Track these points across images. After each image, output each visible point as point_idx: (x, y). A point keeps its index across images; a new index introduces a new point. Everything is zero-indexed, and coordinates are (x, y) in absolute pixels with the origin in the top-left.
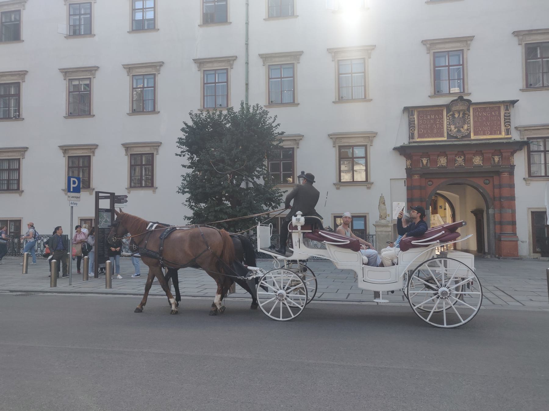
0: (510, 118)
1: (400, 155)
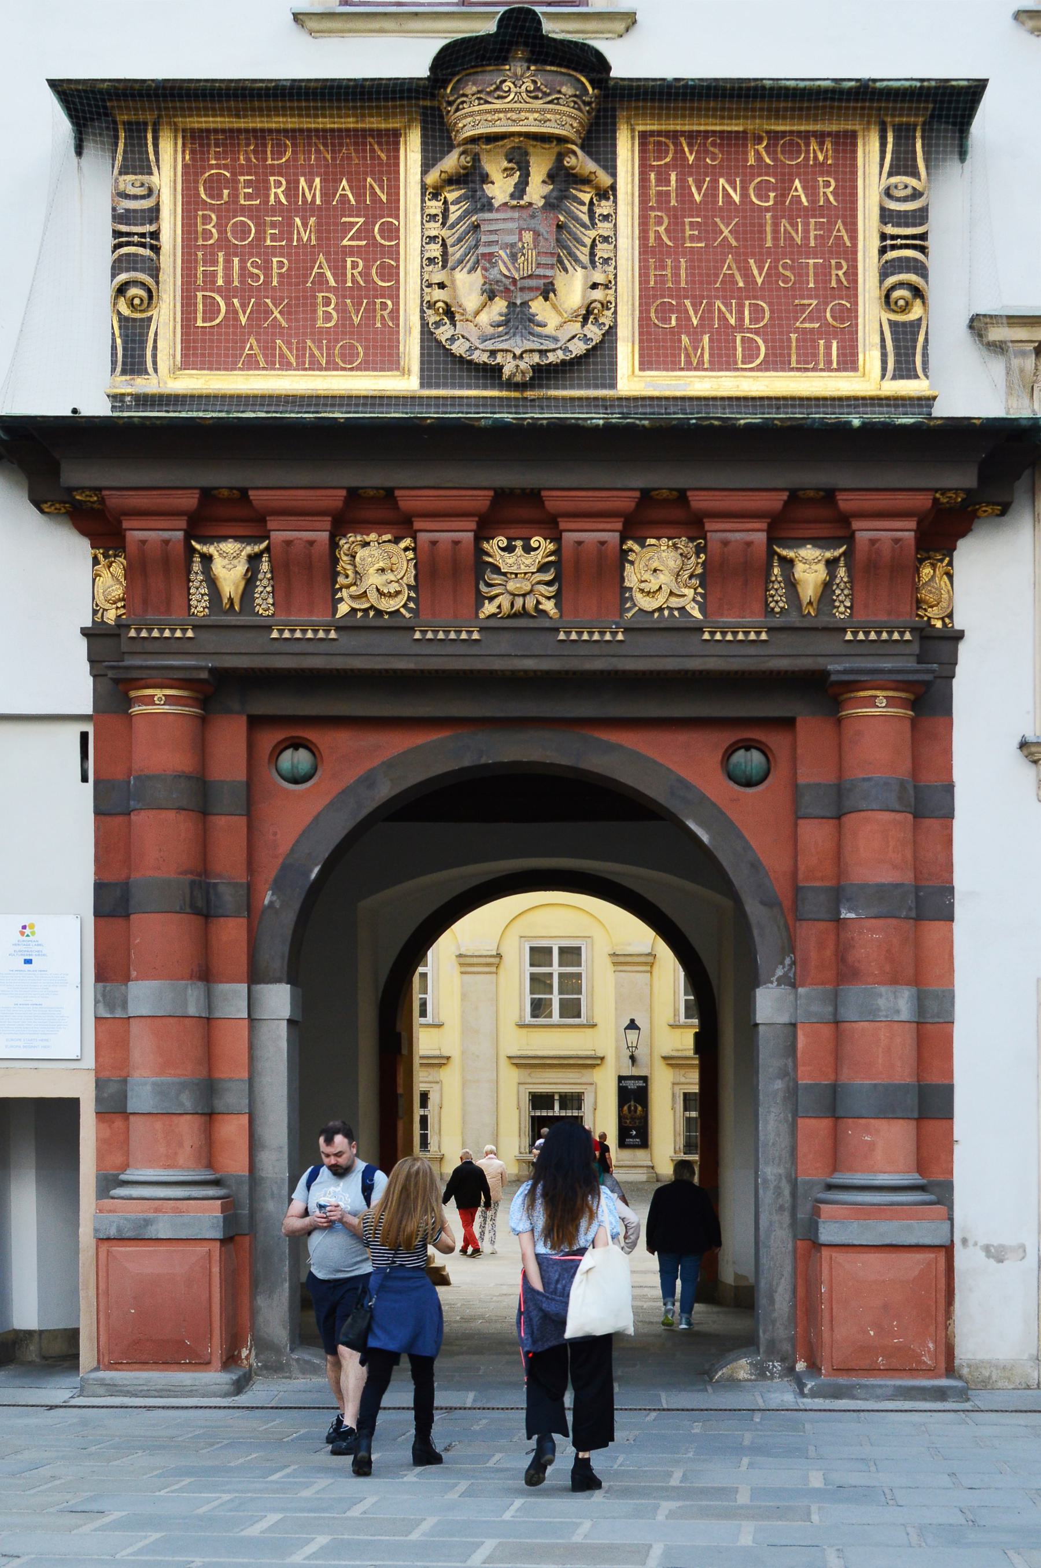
0: (923, 237)
1: (37, 503)
